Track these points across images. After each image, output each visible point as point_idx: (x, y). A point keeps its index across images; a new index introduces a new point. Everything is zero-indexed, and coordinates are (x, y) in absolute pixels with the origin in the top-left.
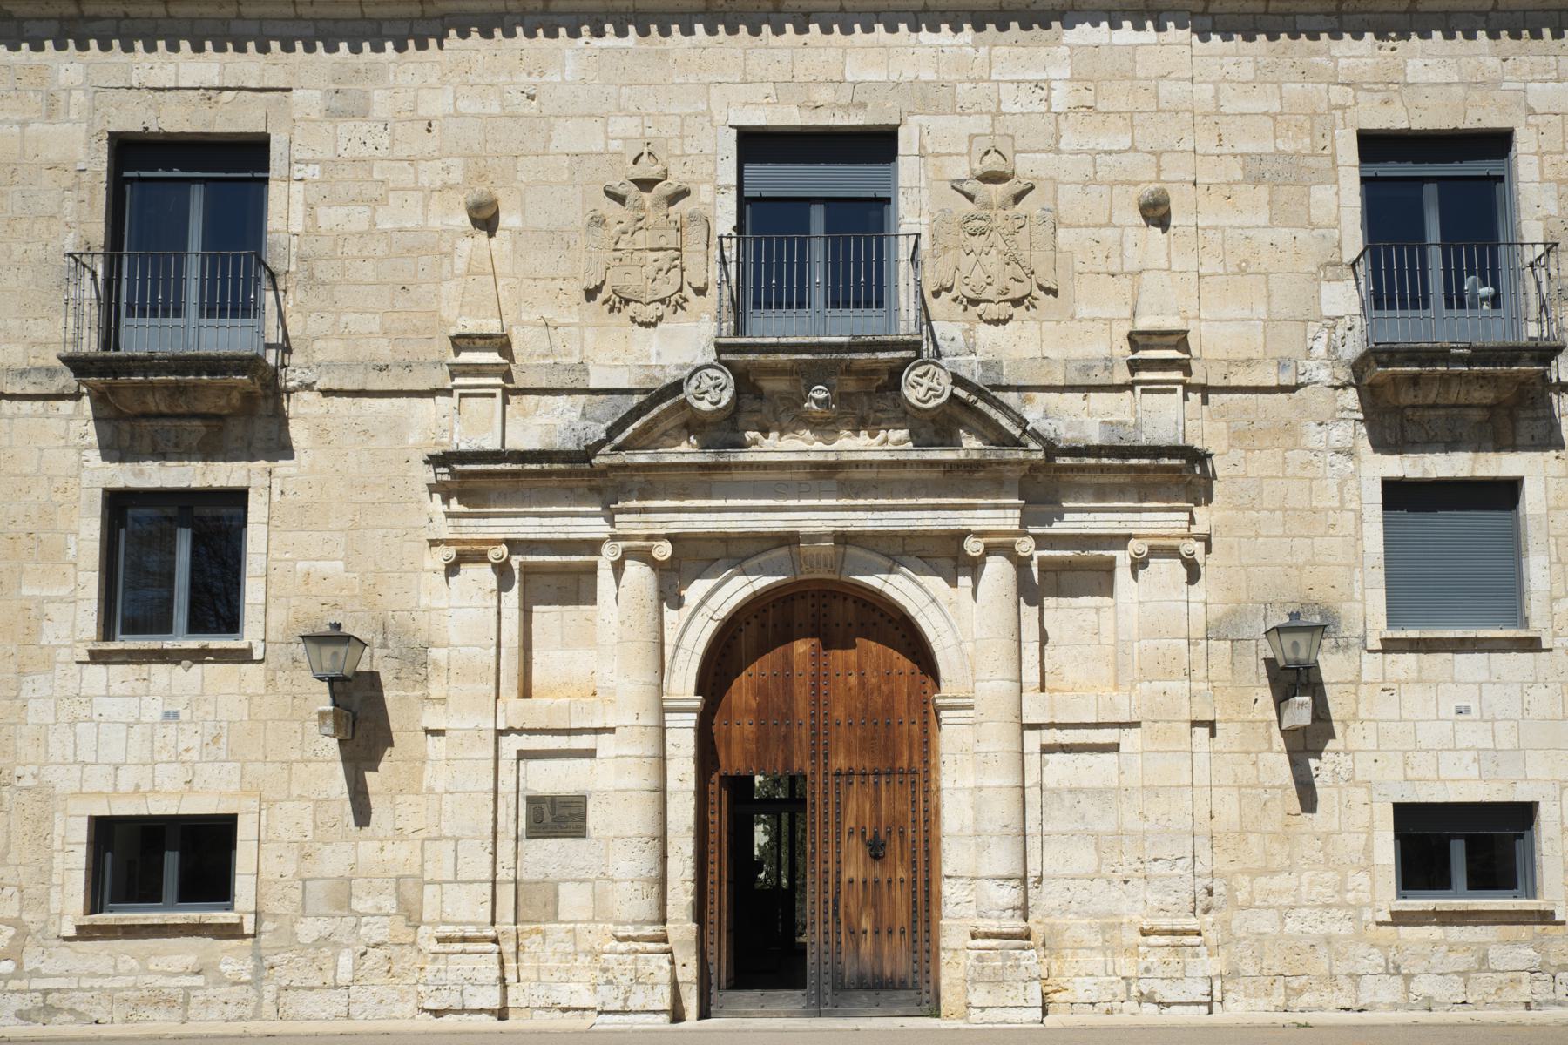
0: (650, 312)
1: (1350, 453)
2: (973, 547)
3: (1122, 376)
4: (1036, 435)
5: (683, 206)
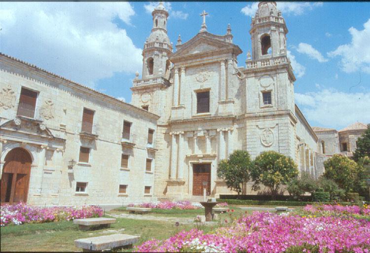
0: (6, 108)
1: (78, 142)
2: (42, 147)
3: (59, 129)
4: (52, 135)
5: (14, 94)
